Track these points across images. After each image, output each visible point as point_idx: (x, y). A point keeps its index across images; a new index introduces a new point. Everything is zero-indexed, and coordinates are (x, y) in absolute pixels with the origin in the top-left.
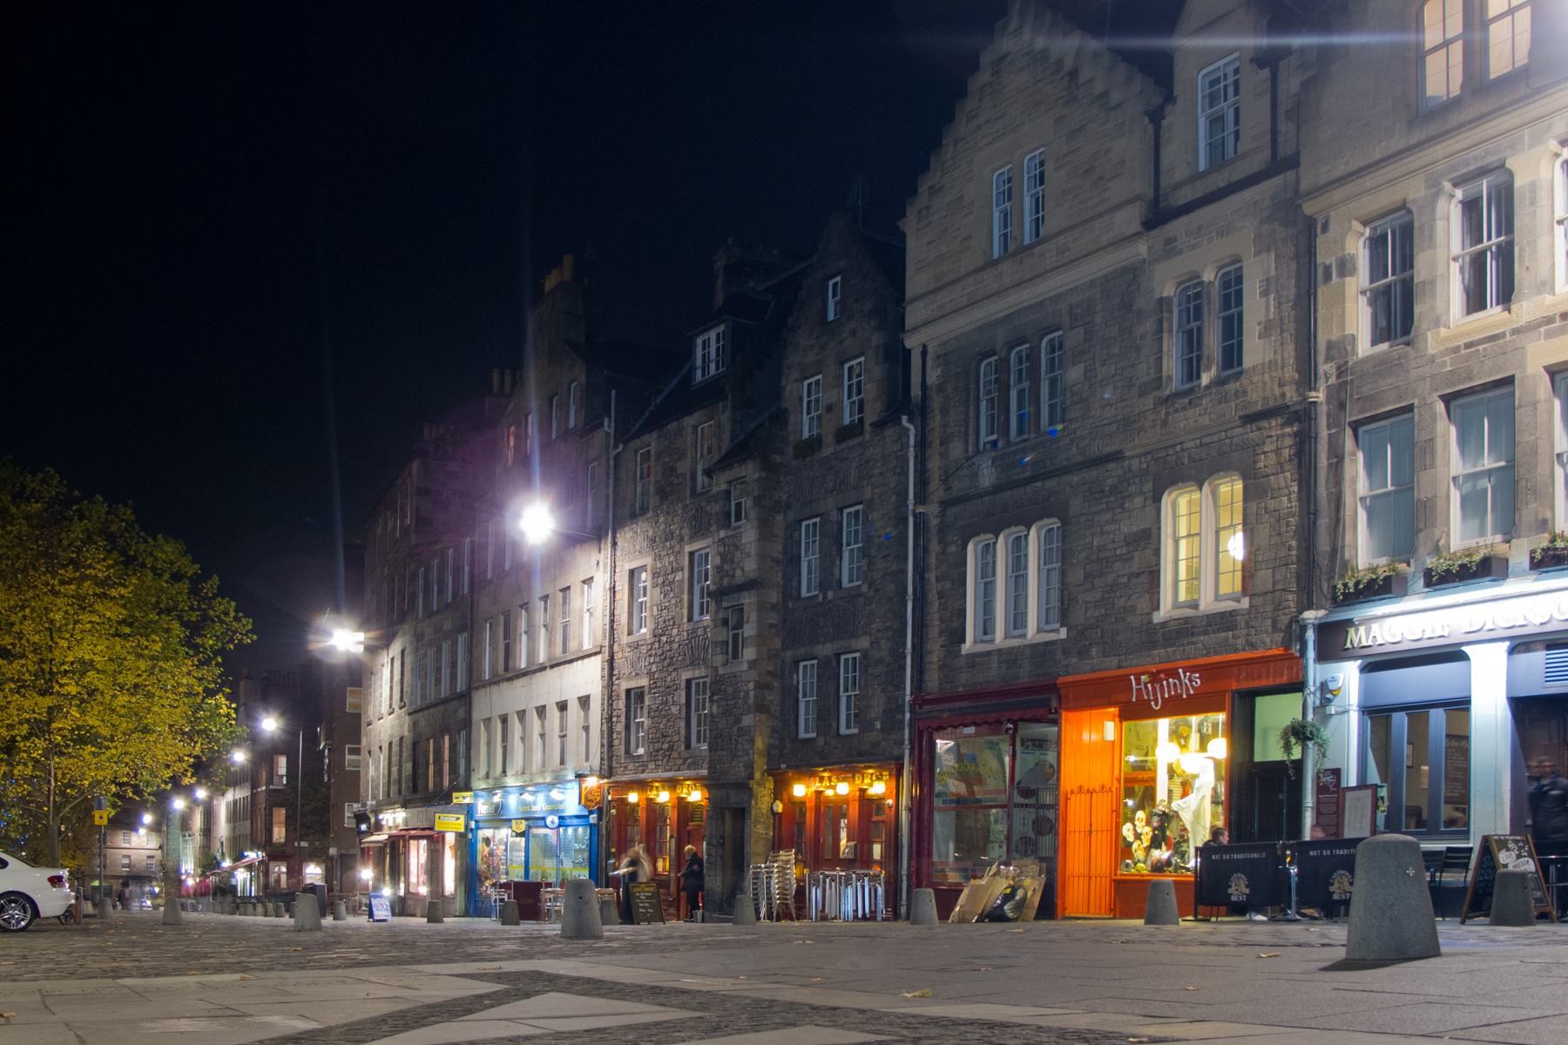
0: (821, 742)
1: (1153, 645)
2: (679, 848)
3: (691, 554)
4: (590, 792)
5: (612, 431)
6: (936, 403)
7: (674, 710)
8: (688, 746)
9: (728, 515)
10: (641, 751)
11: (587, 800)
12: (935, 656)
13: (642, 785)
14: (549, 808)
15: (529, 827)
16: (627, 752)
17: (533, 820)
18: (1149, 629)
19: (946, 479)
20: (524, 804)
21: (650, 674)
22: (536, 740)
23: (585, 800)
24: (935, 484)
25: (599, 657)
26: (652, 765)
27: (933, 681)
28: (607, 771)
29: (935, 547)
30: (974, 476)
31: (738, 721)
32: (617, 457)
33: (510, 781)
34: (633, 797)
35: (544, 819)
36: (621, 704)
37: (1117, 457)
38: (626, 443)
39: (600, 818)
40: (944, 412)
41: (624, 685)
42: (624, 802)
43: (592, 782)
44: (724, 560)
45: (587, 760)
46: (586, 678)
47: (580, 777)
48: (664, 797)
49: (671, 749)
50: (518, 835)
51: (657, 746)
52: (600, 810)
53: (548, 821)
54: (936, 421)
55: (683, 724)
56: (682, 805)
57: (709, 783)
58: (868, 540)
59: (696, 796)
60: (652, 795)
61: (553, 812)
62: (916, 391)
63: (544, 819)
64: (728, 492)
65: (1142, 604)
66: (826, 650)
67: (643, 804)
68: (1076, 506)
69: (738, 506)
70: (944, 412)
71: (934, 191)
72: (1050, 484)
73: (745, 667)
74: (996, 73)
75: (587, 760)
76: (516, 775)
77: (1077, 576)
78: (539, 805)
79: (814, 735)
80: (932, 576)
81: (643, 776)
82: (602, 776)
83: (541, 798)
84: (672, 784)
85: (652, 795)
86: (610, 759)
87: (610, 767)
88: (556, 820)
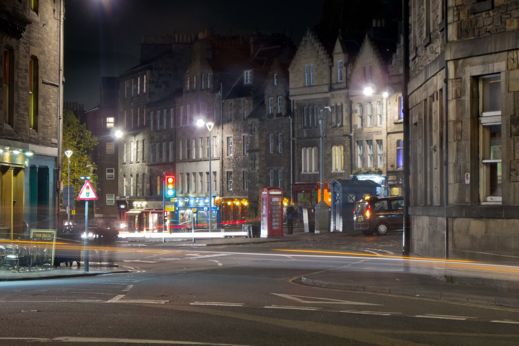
1: (331, 177)
2: (242, 216)
3: (244, 136)
4: (217, 201)
5: (221, 95)
6: (296, 114)
7: (240, 179)
9: (252, 130)
10: (231, 189)
11: (216, 203)
12: (296, 174)
13: (232, 200)
14: (204, 205)
15: (197, 210)
16: (228, 189)
17: (199, 208)
18: (331, 174)
20: (196, 203)
21: (233, 168)
22: (200, 183)
23: (216, 204)
24: (296, 133)
25: (219, 161)
26: (234, 194)
28: (222, 195)
30: (303, 133)
31: (255, 185)
33: (191, 195)
34: (229, 203)
35: (203, 208)
36: (225, 175)
39: (220, 209)
41: (226, 170)
42: (226, 204)
43: (218, 198)
44: (251, 142)
45: (216, 190)
46: (216, 166)
47: (214, 197)
48: (238, 203)
50: (194, 213)
52: (220, 207)
53: (204, 209)
54: (296, 118)
55: (242, 183)
56: (242, 206)
57: (249, 200)
59: (246, 203)
60: (235, 202)
61: (206, 206)
62: (292, 110)
63: (203, 208)
64: (252, 125)
66: (275, 168)
67: (232, 205)
69: (254, 128)
71: (295, 65)
72: (315, 139)
73: (256, 171)
74: (305, 43)
75: (216, 190)
76: (193, 193)
78: (201, 204)
81: (232, 197)
82: (220, 196)
83: (201, 201)
84: (240, 200)
85: (235, 202)
86: (223, 191)
87: (223, 194)
88: (207, 208)
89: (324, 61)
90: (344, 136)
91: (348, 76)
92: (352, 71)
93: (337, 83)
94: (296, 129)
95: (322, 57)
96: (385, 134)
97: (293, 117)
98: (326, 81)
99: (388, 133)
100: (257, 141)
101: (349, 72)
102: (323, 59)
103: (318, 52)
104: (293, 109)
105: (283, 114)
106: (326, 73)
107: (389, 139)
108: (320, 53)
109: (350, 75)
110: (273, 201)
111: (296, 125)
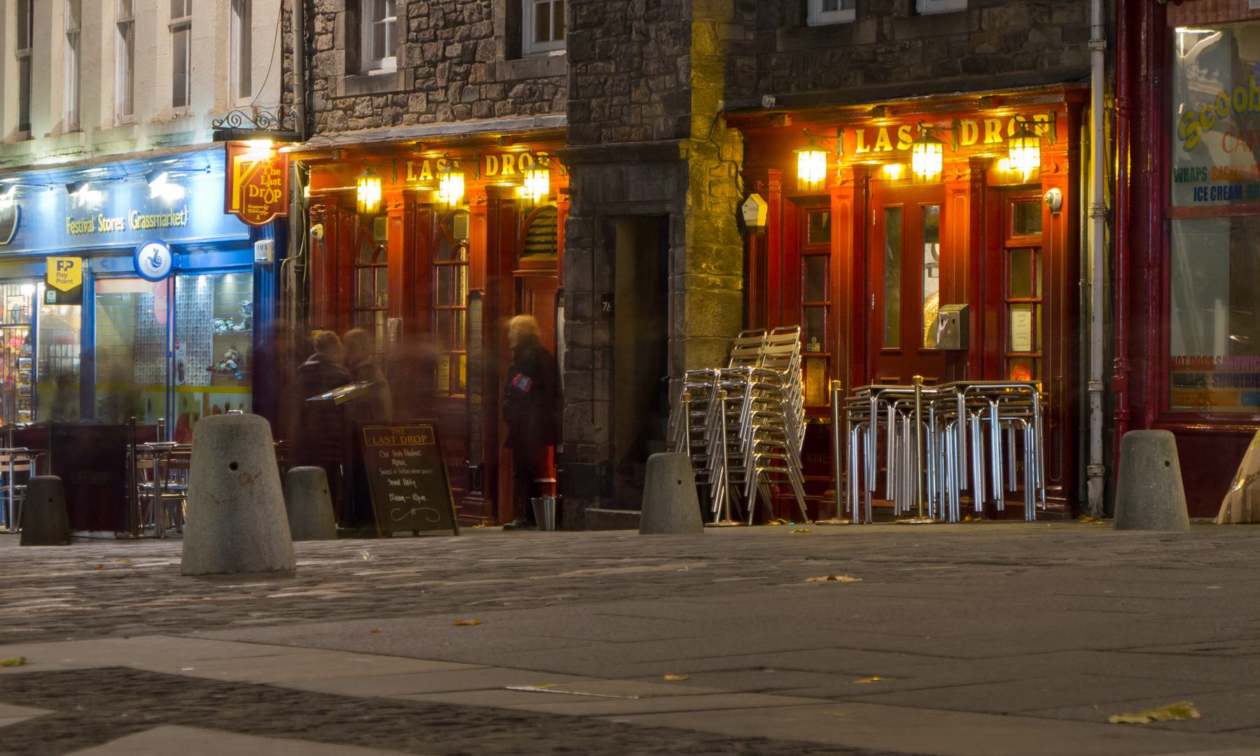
0: (868, 33)
2: (494, 315)
4: (255, 179)
8: (514, 50)
10: (389, 64)
11: (247, 200)
13: (391, 158)
14: (146, 222)
15: (93, 277)
16: (353, 67)
17: (102, 258)
20: (79, 214)
22: (110, 41)
23: (241, 199)
26: (417, 104)
28: (300, 122)
33: (43, 152)
34: (369, 193)
35: (132, 252)
39: (281, 250)
42: (346, 203)
43: (259, 152)
45: (246, 90)
47: (227, 137)
48: (451, 190)
49: (469, 57)
50: (63, 298)
51: (432, 50)
52: (282, 230)
53: (146, 254)
56: (500, 212)
57: (574, 150)
59: (536, 187)
60: (419, 183)
61: (155, 234)
63: (132, 252)
67: (397, 207)
75: (246, 90)
76: (58, 134)
78: (117, 211)
79: (848, 15)
81: (394, 132)
82: (285, 135)
83: (123, 194)
84: (471, 153)
85: (419, 183)
86: (307, 87)
87: (308, 110)
88: (164, 253)
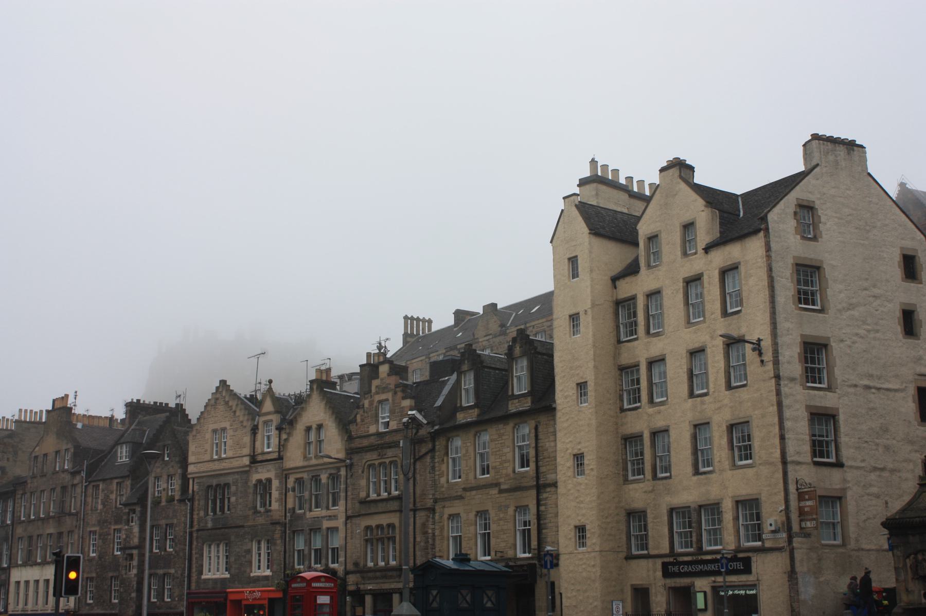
6: (197, 497)
9: (128, 521)
18: (249, 577)
19: (199, 522)
24: (195, 523)
27: (193, 586)
29: (195, 543)
32: (86, 487)
37: (243, 526)
38: (90, 482)
40: (199, 500)
54: (196, 503)
58: (175, 537)
62: (190, 491)
65: (248, 570)
68: (233, 538)
70: (199, 500)
77: (232, 559)
80: (194, 552)
89: (245, 424)
90: (273, 524)
91: (282, 443)
92: (289, 434)
93: (263, 453)
94: (195, 517)
95: (241, 419)
96: (342, 519)
97: (192, 500)
98: (247, 451)
99: (348, 518)
100: (137, 535)
101: (284, 436)
102: (242, 422)
103: (235, 412)
104: (193, 491)
105: (177, 498)
106: (247, 439)
107: (349, 526)
108: (237, 414)
109: (286, 440)
110: (318, 602)
111: (195, 513)
